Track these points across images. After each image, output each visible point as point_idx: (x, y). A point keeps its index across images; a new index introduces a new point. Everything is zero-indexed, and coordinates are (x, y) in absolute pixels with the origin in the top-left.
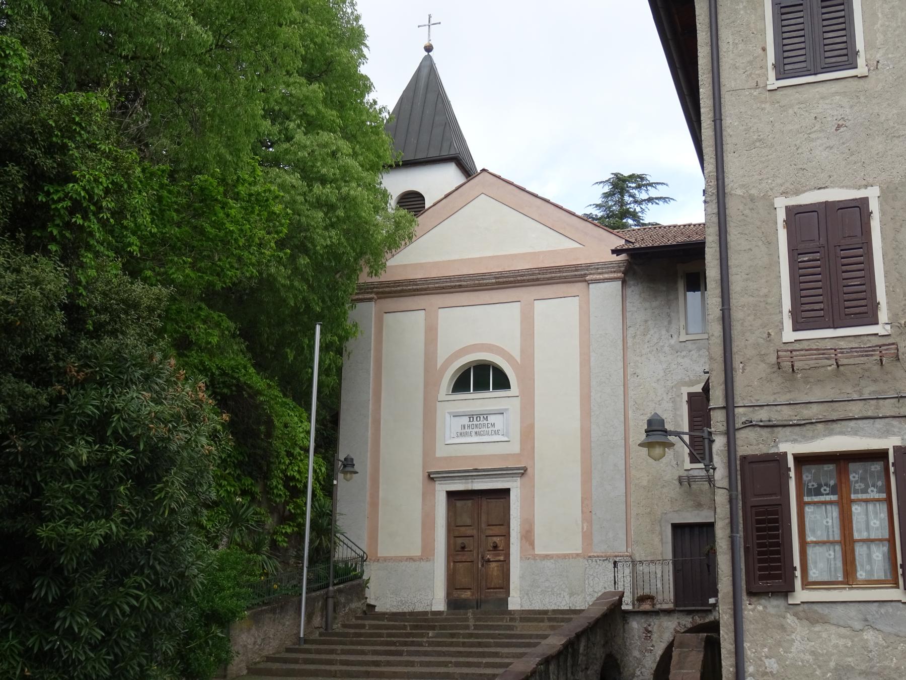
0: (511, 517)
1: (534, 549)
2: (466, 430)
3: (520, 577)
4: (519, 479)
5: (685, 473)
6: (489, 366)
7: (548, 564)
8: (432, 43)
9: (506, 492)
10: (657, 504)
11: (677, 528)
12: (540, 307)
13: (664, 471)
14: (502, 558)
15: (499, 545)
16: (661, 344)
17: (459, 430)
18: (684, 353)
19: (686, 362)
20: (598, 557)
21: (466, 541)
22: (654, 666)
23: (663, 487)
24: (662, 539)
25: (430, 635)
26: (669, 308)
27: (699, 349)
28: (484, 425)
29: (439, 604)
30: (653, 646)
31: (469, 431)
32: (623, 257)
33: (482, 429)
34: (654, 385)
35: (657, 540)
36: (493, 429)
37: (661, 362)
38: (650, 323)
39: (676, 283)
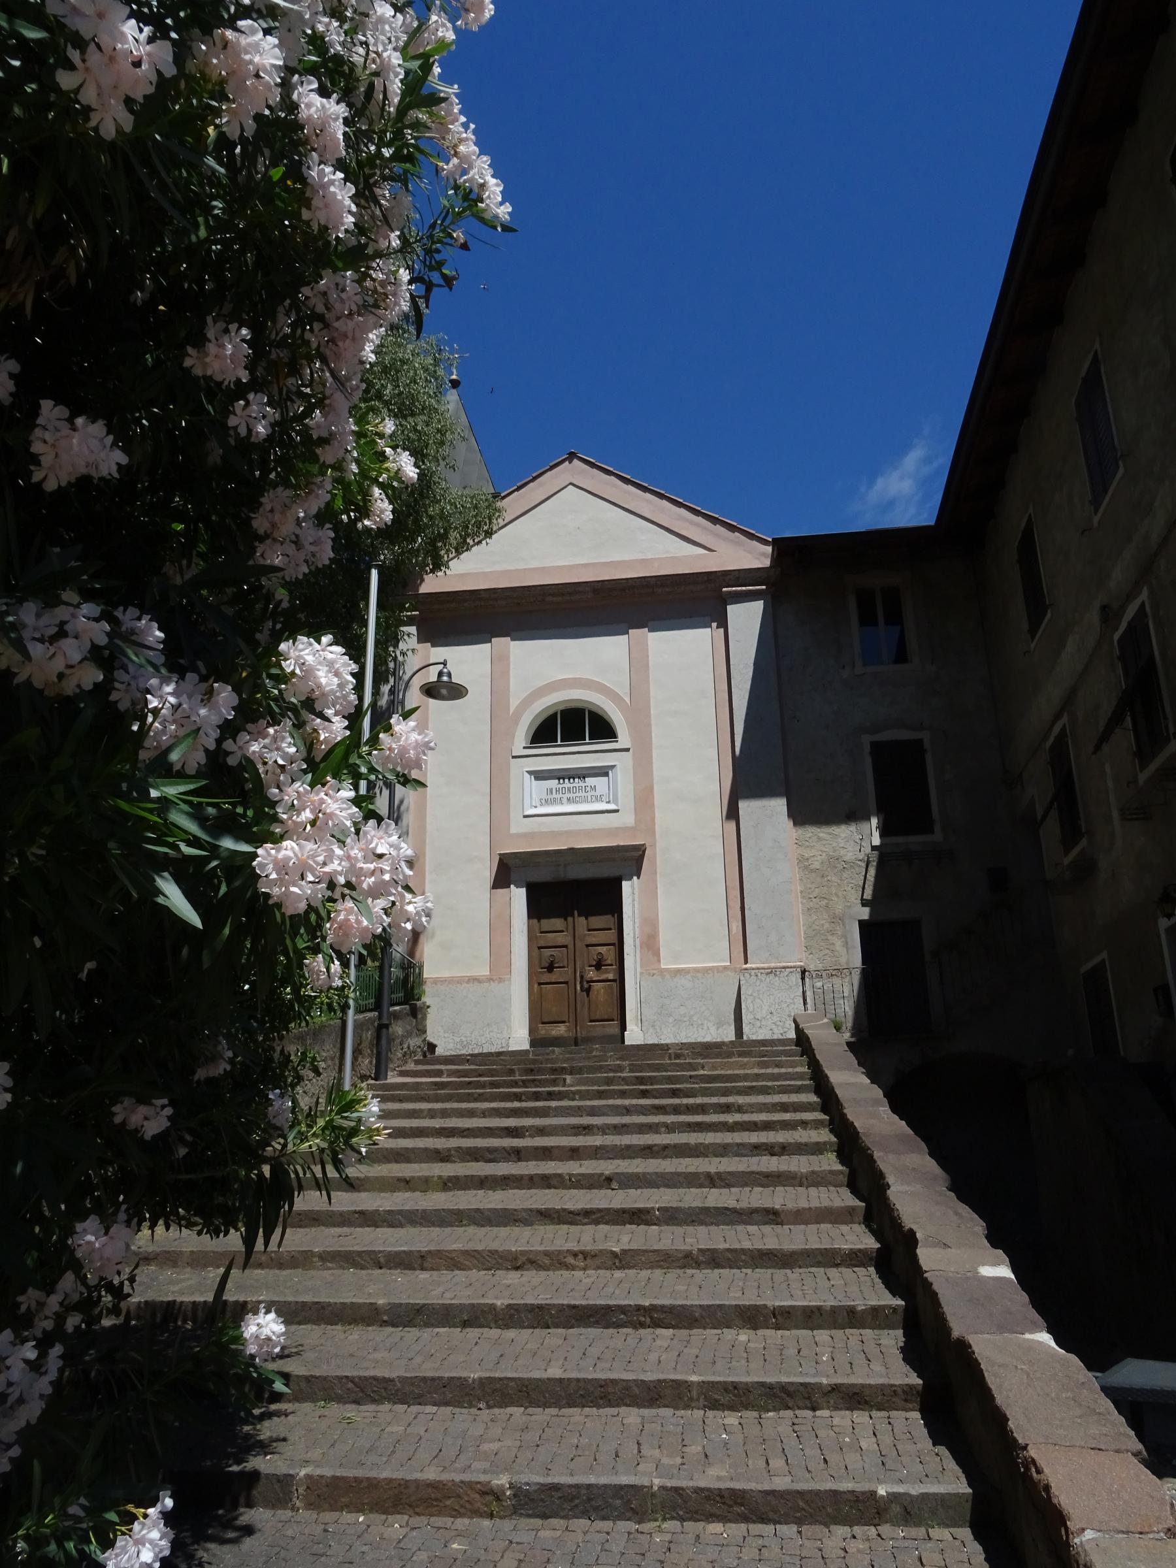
1: (659, 961)
2: (554, 795)
7: (683, 981)
10: (836, 894)
14: (611, 976)
15: (605, 957)
17: (544, 796)
20: (758, 969)
25: (568, 1081)
28: (580, 788)
31: (558, 796)
33: (577, 794)
36: (593, 793)
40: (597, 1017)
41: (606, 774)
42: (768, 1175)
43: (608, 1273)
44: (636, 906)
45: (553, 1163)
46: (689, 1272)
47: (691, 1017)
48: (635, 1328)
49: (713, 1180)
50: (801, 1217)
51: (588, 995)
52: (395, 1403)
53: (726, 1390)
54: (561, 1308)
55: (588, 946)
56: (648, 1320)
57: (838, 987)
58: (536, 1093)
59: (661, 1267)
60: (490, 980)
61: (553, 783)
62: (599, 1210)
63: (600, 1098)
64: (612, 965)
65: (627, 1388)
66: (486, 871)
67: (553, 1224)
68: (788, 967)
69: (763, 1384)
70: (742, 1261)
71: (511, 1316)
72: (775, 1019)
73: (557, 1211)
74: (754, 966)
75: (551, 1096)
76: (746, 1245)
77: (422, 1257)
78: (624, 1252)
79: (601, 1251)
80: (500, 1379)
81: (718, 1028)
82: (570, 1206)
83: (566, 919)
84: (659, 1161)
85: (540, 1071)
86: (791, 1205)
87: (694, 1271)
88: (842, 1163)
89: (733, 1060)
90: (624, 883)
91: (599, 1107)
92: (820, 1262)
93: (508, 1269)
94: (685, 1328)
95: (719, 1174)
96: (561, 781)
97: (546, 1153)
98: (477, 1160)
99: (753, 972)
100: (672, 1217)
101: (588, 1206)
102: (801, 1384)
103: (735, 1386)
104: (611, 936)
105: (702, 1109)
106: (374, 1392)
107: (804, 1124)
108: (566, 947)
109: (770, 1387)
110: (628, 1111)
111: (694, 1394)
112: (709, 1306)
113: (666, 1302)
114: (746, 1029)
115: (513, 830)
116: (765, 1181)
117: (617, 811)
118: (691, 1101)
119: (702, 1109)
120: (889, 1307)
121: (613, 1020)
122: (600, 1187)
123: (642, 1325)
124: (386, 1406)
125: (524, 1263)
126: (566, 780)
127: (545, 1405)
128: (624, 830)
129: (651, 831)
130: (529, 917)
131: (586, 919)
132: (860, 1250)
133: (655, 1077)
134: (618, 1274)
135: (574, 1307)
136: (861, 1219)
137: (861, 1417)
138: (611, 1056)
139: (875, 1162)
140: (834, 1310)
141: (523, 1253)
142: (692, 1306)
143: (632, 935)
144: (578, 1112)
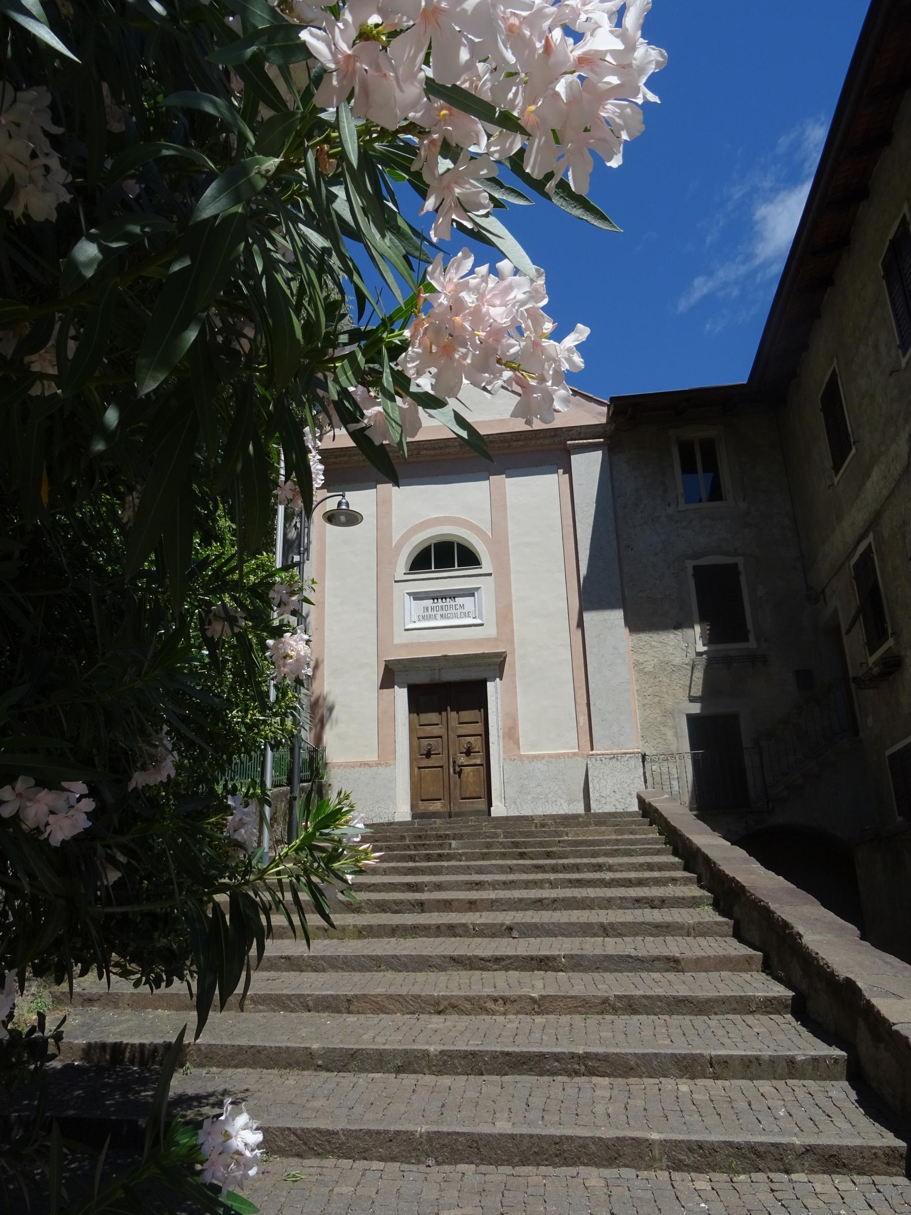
1: (519, 748)
2: (430, 613)
6: (453, 543)
14: (478, 761)
15: (474, 745)
20: (602, 755)
21: (431, 741)
24: (677, 733)
25: (453, 845)
31: (433, 613)
35: (670, 734)
36: (462, 610)
40: (468, 796)
41: (473, 595)
42: (657, 926)
43: (529, 1018)
44: (499, 703)
45: (454, 915)
46: (609, 1017)
48: (569, 1075)
49: (606, 930)
50: (701, 965)
51: (460, 777)
52: (339, 1157)
53: (691, 1150)
54: (494, 1055)
55: (459, 736)
56: (583, 1068)
57: (664, 769)
58: (428, 854)
59: (580, 1013)
60: (378, 764)
61: (429, 603)
62: (509, 957)
63: (483, 859)
64: (479, 752)
65: (585, 1146)
66: (375, 675)
67: (466, 969)
68: (627, 753)
69: (730, 1144)
70: (659, 1007)
71: (445, 1063)
72: (618, 796)
73: (469, 958)
74: (599, 752)
75: (440, 857)
76: (659, 991)
77: (349, 1001)
78: (543, 997)
79: (520, 997)
80: (449, 1134)
81: (569, 804)
82: (480, 953)
83: (440, 714)
84: (550, 912)
85: (427, 837)
86: (688, 954)
87: (612, 1017)
88: (723, 913)
89: (591, 828)
90: (490, 686)
91: (486, 866)
92: (735, 1009)
93: (430, 1013)
94: (621, 1076)
95: (611, 925)
96: (436, 600)
97: (447, 906)
98: (385, 911)
99: (598, 757)
100: (577, 964)
101: (497, 953)
102: (773, 1145)
103: (700, 1145)
104: (478, 728)
105: (577, 868)
106: (317, 1144)
107: (674, 880)
108: (441, 737)
109: (738, 1147)
110: (511, 869)
111: (656, 1153)
112: (644, 1055)
113: (601, 1050)
114: (593, 805)
115: (396, 641)
116: (655, 931)
117: (482, 625)
118: (565, 861)
119: (577, 868)
120: (830, 1057)
121: (480, 798)
122: (502, 936)
123: (577, 1073)
124: (330, 1162)
125: (446, 1008)
126: (440, 600)
127: (498, 1163)
128: (489, 640)
129: (511, 642)
130: (410, 712)
131: (457, 713)
132: (774, 998)
133: (528, 842)
134: (539, 1019)
135: (508, 1054)
136: (760, 967)
137: (842, 1182)
138: (486, 825)
139: (773, 913)
140: (773, 1061)
141: (445, 998)
142: (627, 1054)
143: (496, 727)
144: (467, 870)
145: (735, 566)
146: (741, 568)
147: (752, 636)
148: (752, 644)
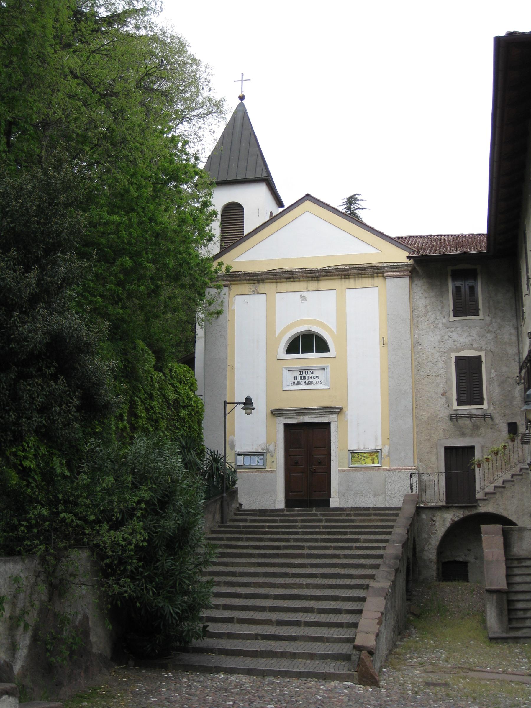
0: (331, 442)
2: (298, 380)
3: (338, 484)
4: (337, 415)
5: (454, 413)
8: (243, 93)
9: (328, 424)
10: (434, 434)
11: (448, 450)
12: (350, 293)
13: (439, 411)
16: (436, 322)
18: (453, 329)
19: (455, 335)
22: (438, 543)
23: (438, 422)
26: (442, 297)
27: (463, 327)
28: (311, 377)
29: (280, 503)
30: (436, 530)
31: (300, 381)
32: (412, 260)
34: (432, 351)
35: (434, 458)
37: (436, 335)
38: (428, 307)
39: (446, 280)
47: (362, 492)
145: (480, 357)
146: (483, 359)
147: (485, 402)
148: (485, 406)
